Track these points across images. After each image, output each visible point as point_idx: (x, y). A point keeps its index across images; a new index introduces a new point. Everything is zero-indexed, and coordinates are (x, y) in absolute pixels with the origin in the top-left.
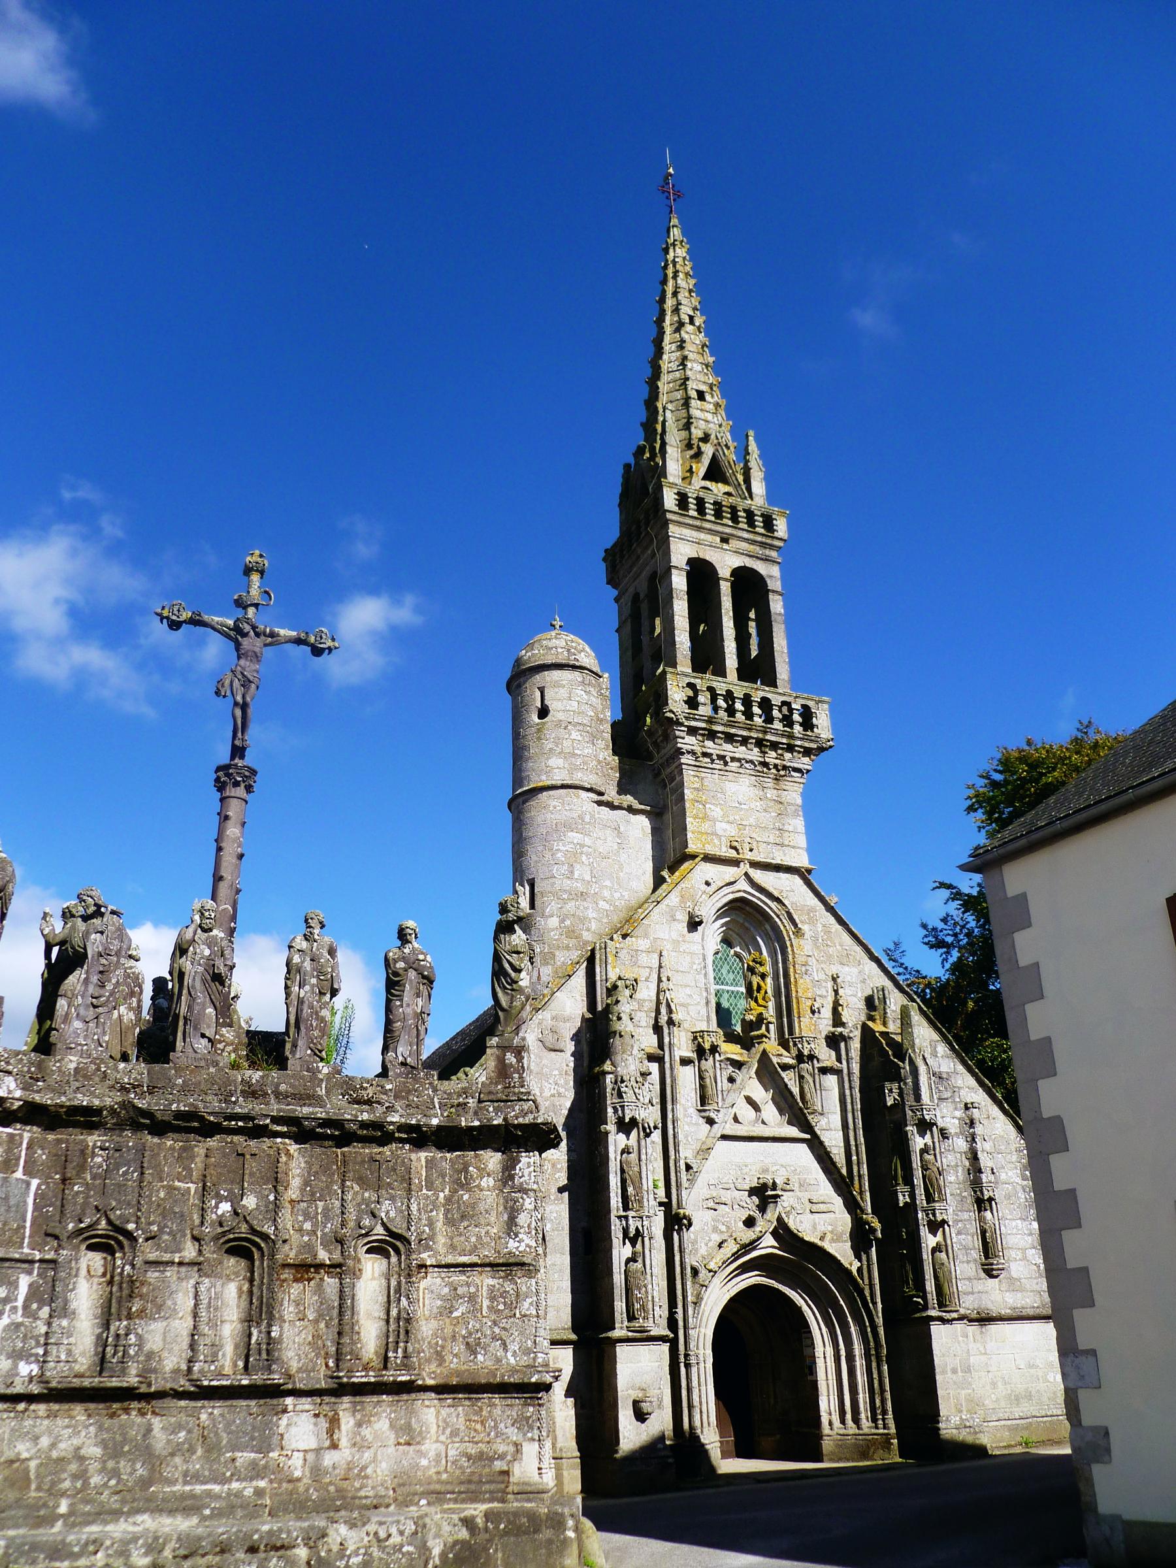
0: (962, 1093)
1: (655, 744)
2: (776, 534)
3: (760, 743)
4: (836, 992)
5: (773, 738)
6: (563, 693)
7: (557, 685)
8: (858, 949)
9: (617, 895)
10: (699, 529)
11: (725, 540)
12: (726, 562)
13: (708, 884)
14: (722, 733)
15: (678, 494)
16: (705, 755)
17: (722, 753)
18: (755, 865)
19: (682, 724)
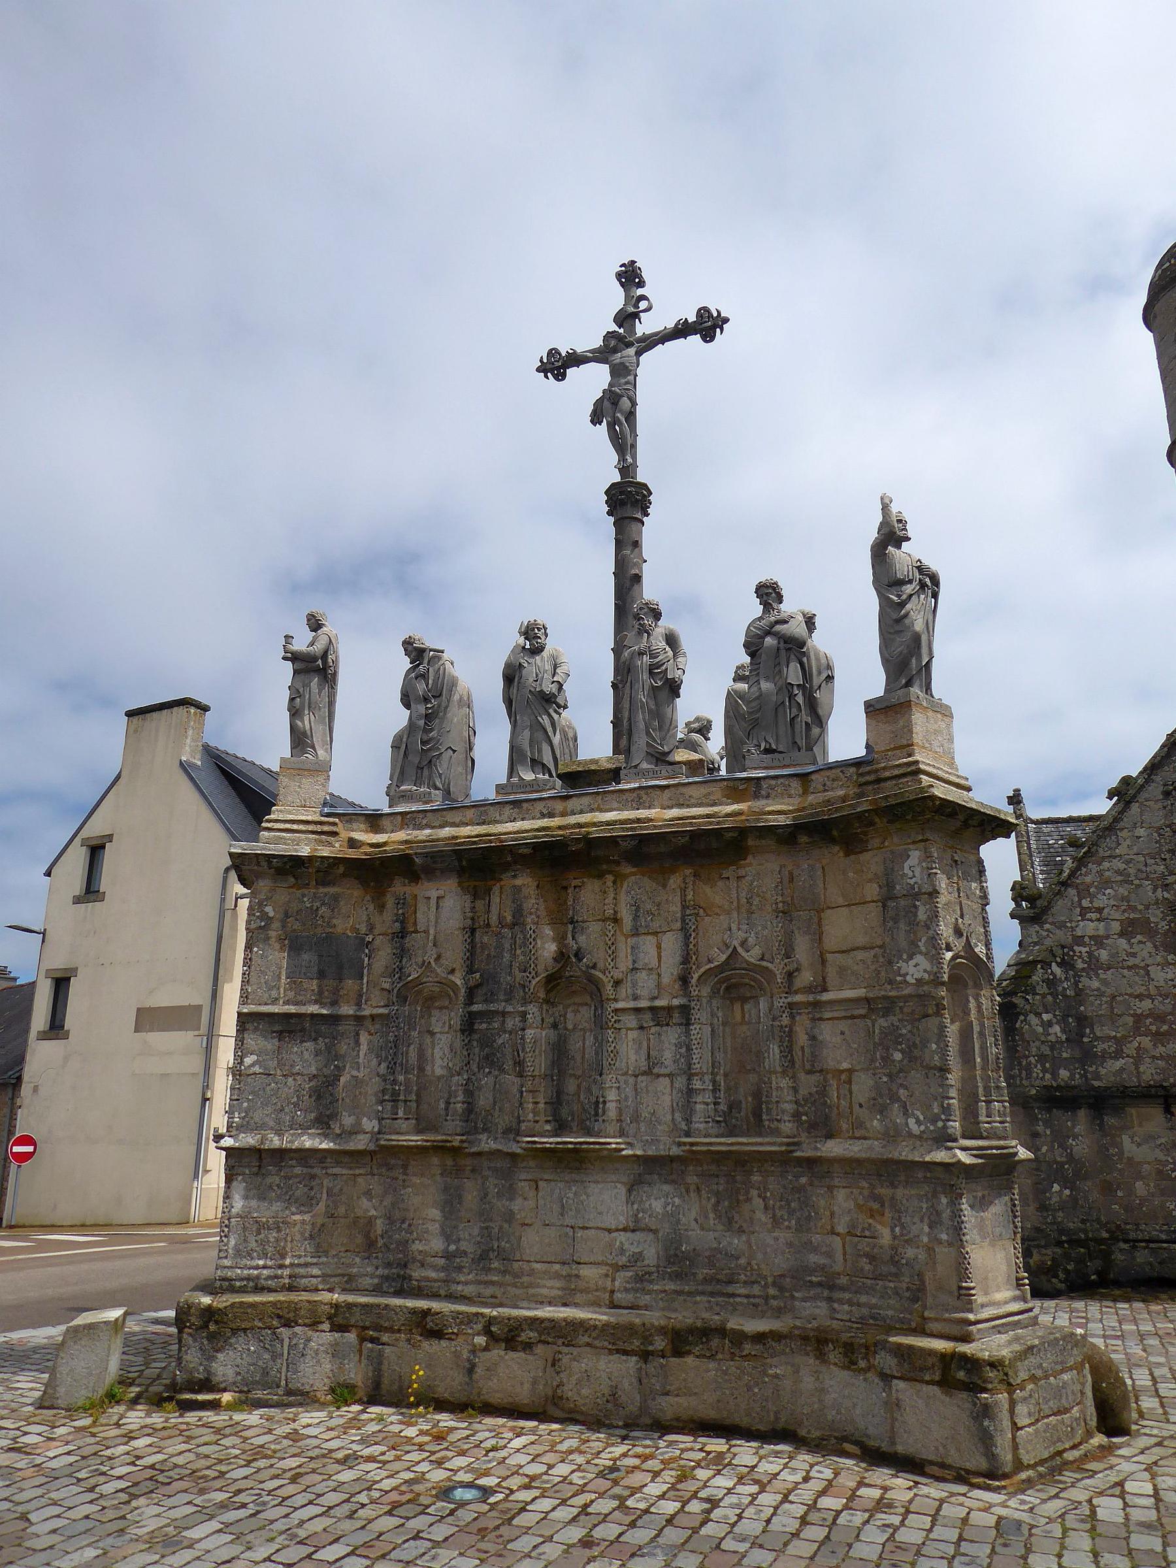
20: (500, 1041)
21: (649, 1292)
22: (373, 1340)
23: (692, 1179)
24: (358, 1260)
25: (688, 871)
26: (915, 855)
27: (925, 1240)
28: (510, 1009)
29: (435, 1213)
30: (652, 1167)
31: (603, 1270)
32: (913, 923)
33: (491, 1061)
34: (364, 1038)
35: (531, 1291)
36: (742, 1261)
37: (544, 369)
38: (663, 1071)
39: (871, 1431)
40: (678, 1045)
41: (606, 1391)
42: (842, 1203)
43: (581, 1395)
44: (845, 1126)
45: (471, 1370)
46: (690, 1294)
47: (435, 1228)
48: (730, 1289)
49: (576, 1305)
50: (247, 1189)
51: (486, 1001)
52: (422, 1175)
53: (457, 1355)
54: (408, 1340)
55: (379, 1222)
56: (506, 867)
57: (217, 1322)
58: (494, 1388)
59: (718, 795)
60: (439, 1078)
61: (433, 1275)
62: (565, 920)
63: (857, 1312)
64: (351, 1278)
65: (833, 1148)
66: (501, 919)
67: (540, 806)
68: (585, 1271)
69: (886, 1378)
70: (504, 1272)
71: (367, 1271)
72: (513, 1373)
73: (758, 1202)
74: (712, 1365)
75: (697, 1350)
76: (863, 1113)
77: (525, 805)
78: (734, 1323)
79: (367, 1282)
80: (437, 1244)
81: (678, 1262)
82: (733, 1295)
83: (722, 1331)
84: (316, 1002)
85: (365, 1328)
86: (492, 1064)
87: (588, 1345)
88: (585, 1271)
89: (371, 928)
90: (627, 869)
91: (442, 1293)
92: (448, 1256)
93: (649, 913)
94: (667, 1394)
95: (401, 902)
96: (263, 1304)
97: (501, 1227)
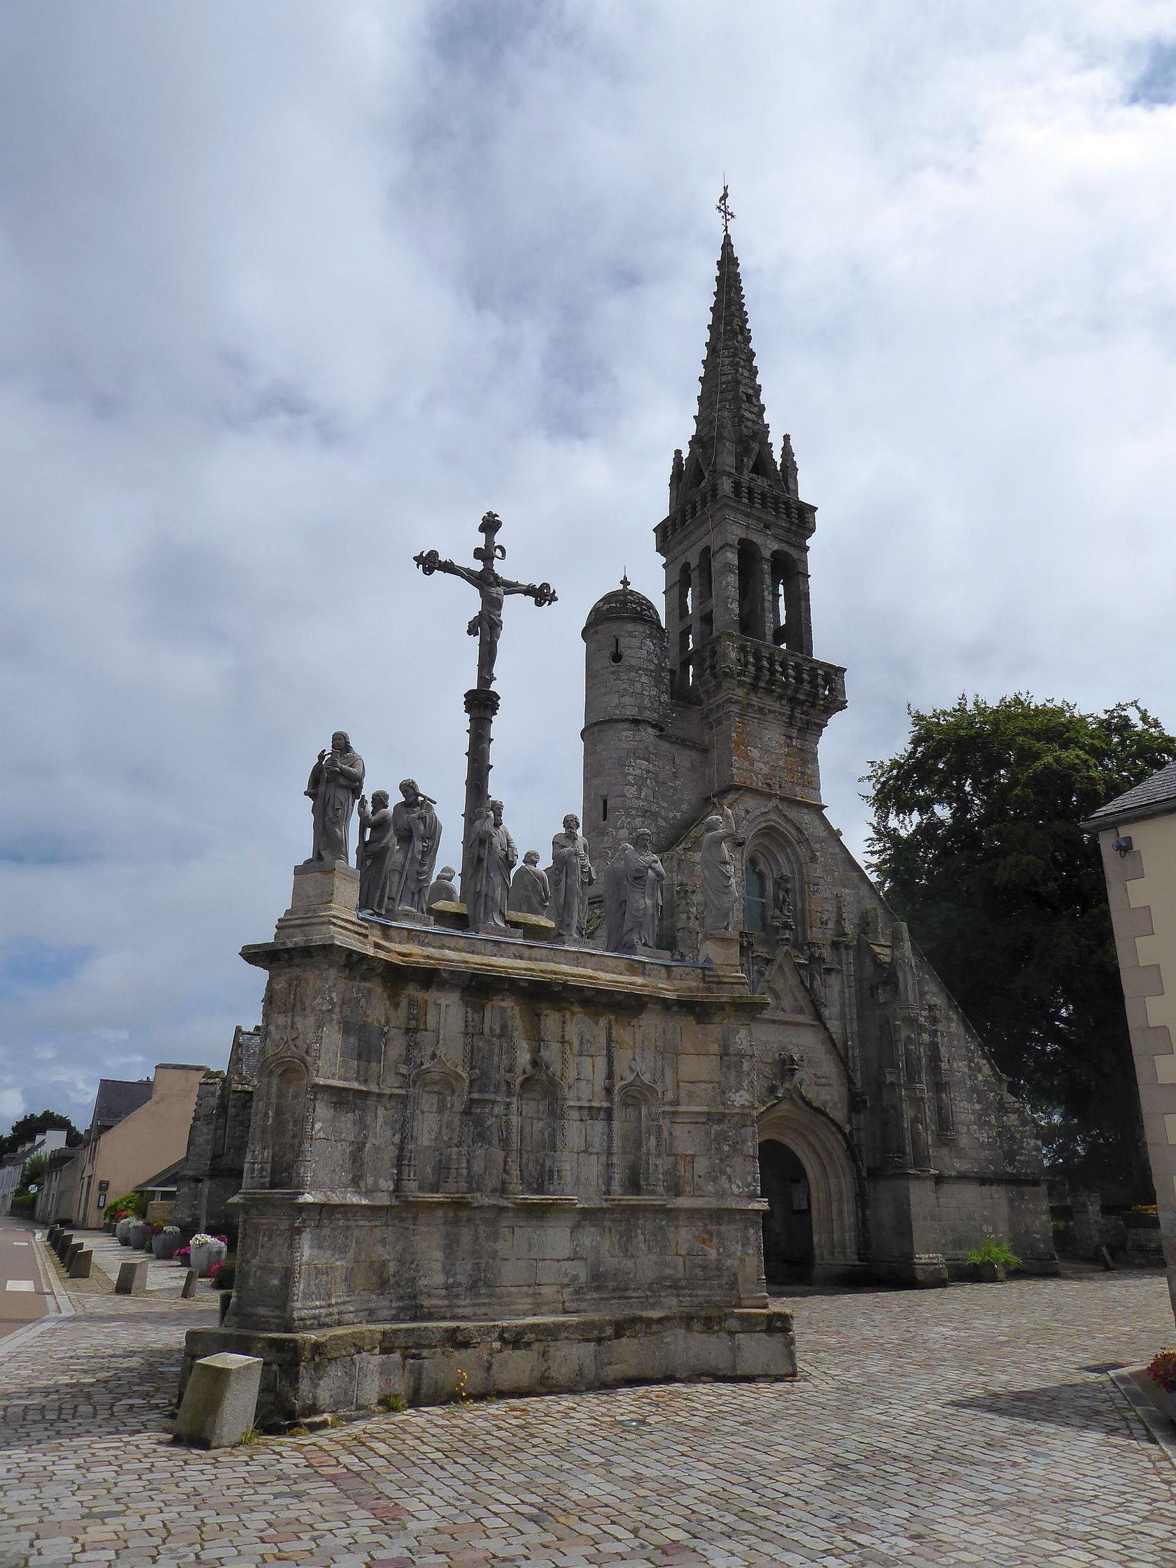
0: (928, 997)
1: (707, 692)
4: (839, 908)
6: (635, 642)
7: (631, 634)
8: (855, 875)
9: (671, 815)
10: (748, 515)
11: (767, 527)
12: (769, 546)
13: (747, 812)
16: (749, 705)
18: (782, 799)
19: (732, 677)
20: (489, 1123)
21: (585, 1301)
22: (414, 1357)
23: (607, 1224)
24: (373, 1297)
25: (612, 1017)
26: (743, 1033)
27: (739, 1254)
28: (499, 1099)
29: (439, 1255)
30: (589, 1215)
31: (555, 1288)
32: (740, 1072)
33: (482, 1137)
34: (381, 1112)
35: (512, 1307)
36: (631, 1276)
37: (419, 559)
38: (594, 1151)
39: (721, 1366)
40: (603, 1134)
41: (577, 1368)
42: (684, 1236)
43: (560, 1372)
44: (688, 1189)
45: (489, 1369)
46: (608, 1299)
47: (438, 1266)
48: (628, 1294)
49: (542, 1314)
50: (312, 1240)
51: (480, 1091)
52: (429, 1225)
53: (480, 1358)
54: (443, 1353)
55: (391, 1264)
56: (498, 991)
57: (320, 1354)
58: (503, 1379)
59: (622, 968)
60: (427, 1147)
61: (440, 1302)
62: (537, 1039)
63: (696, 1301)
64: (371, 1312)
65: (684, 1202)
66: (492, 1031)
67: (513, 949)
68: (545, 1290)
69: (731, 1333)
70: (491, 1295)
71: (384, 1305)
72: (518, 1366)
73: (641, 1237)
74: (636, 1341)
75: (628, 1333)
76: (702, 1181)
77: (503, 946)
78: (645, 1314)
79: (386, 1313)
80: (439, 1279)
81: (598, 1279)
82: (630, 1298)
83: (641, 1319)
84: (357, 1079)
85: (407, 1348)
86: (483, 1140)
87: (567, 1338)
88: (545, 1290)
89: (388, 1021)
90: (577, 1009)
91: (448, 1315)
92: (447, 1287)
93: (589, 1041)
94: (610, 1364)
95: (412, 1003)
96: (346, 1335)
97: (487, 1263)
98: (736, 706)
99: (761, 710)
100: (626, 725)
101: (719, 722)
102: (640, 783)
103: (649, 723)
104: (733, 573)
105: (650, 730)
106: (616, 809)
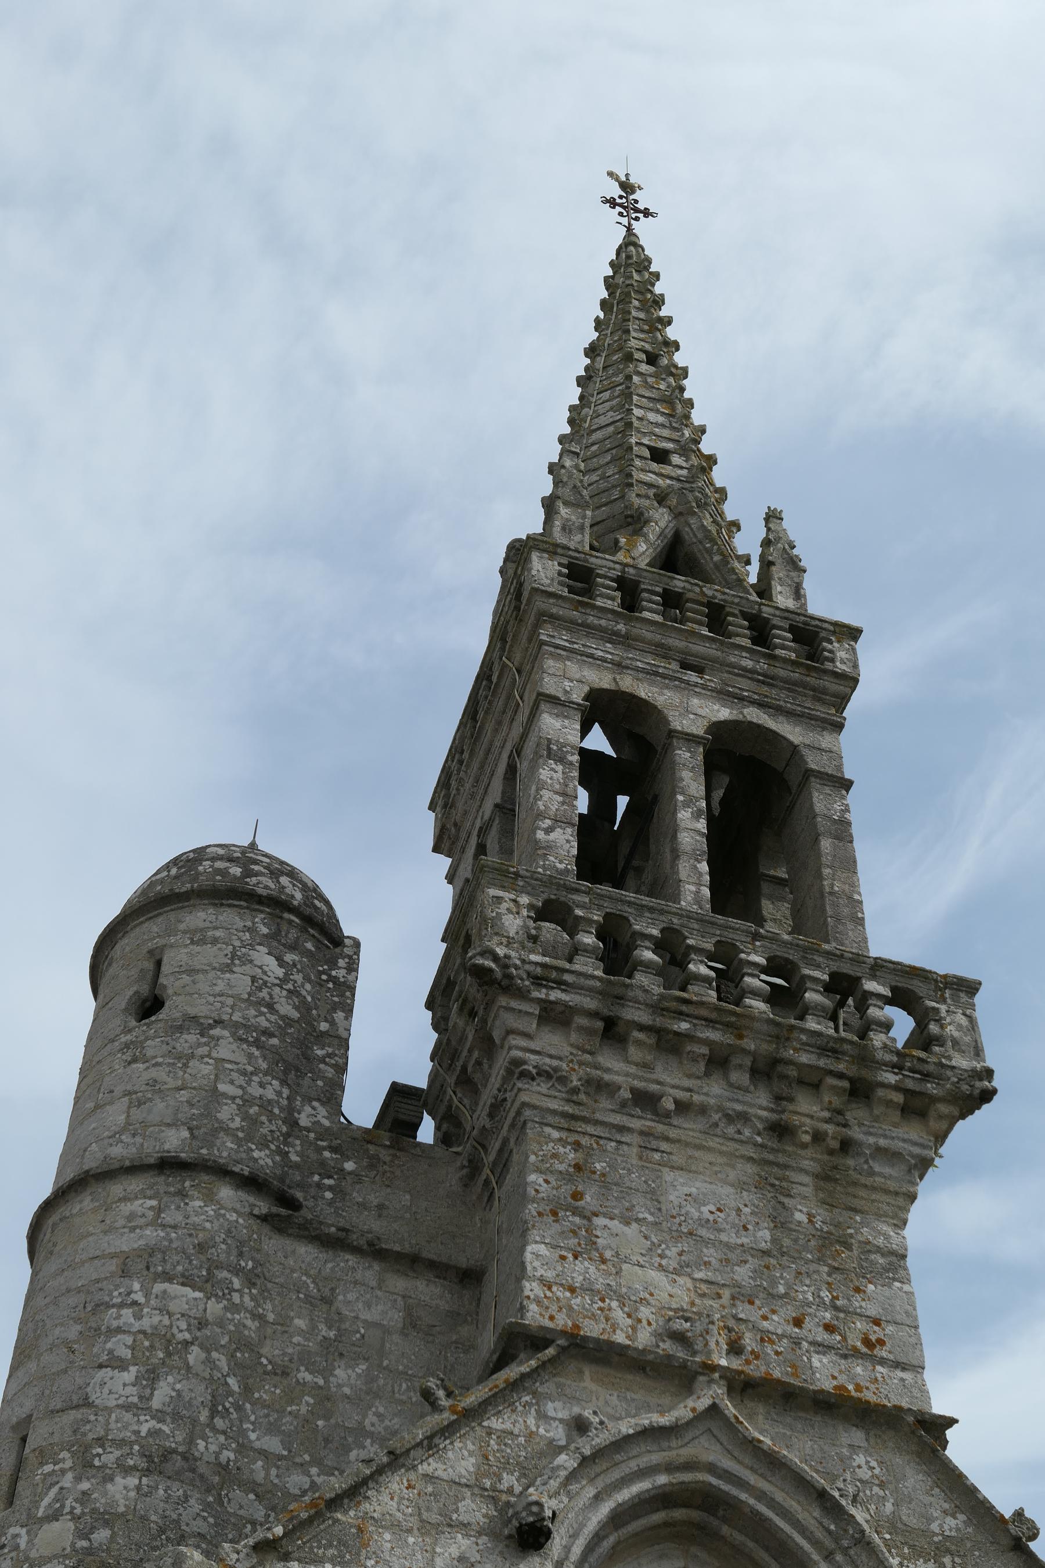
2: (829, 666)
3: (766, 1071)
5: (804, 1058)
6: (211, 954)
7: (198, 937)
10: (625, 641)
12: (693, 711)
14: (642, 1028)
15: (569, 566)
16: (599, 1087)
17: (654, 1087)
19: (522, 994)
98: (544, 1088)
99: (645, 1101)
100: (135, 1184)
101: (502, 1164)
102: (159, 1355)
103: (223, 1172)
104: (561, 760)
105: (226, 1193)
106: (44, 1455)
